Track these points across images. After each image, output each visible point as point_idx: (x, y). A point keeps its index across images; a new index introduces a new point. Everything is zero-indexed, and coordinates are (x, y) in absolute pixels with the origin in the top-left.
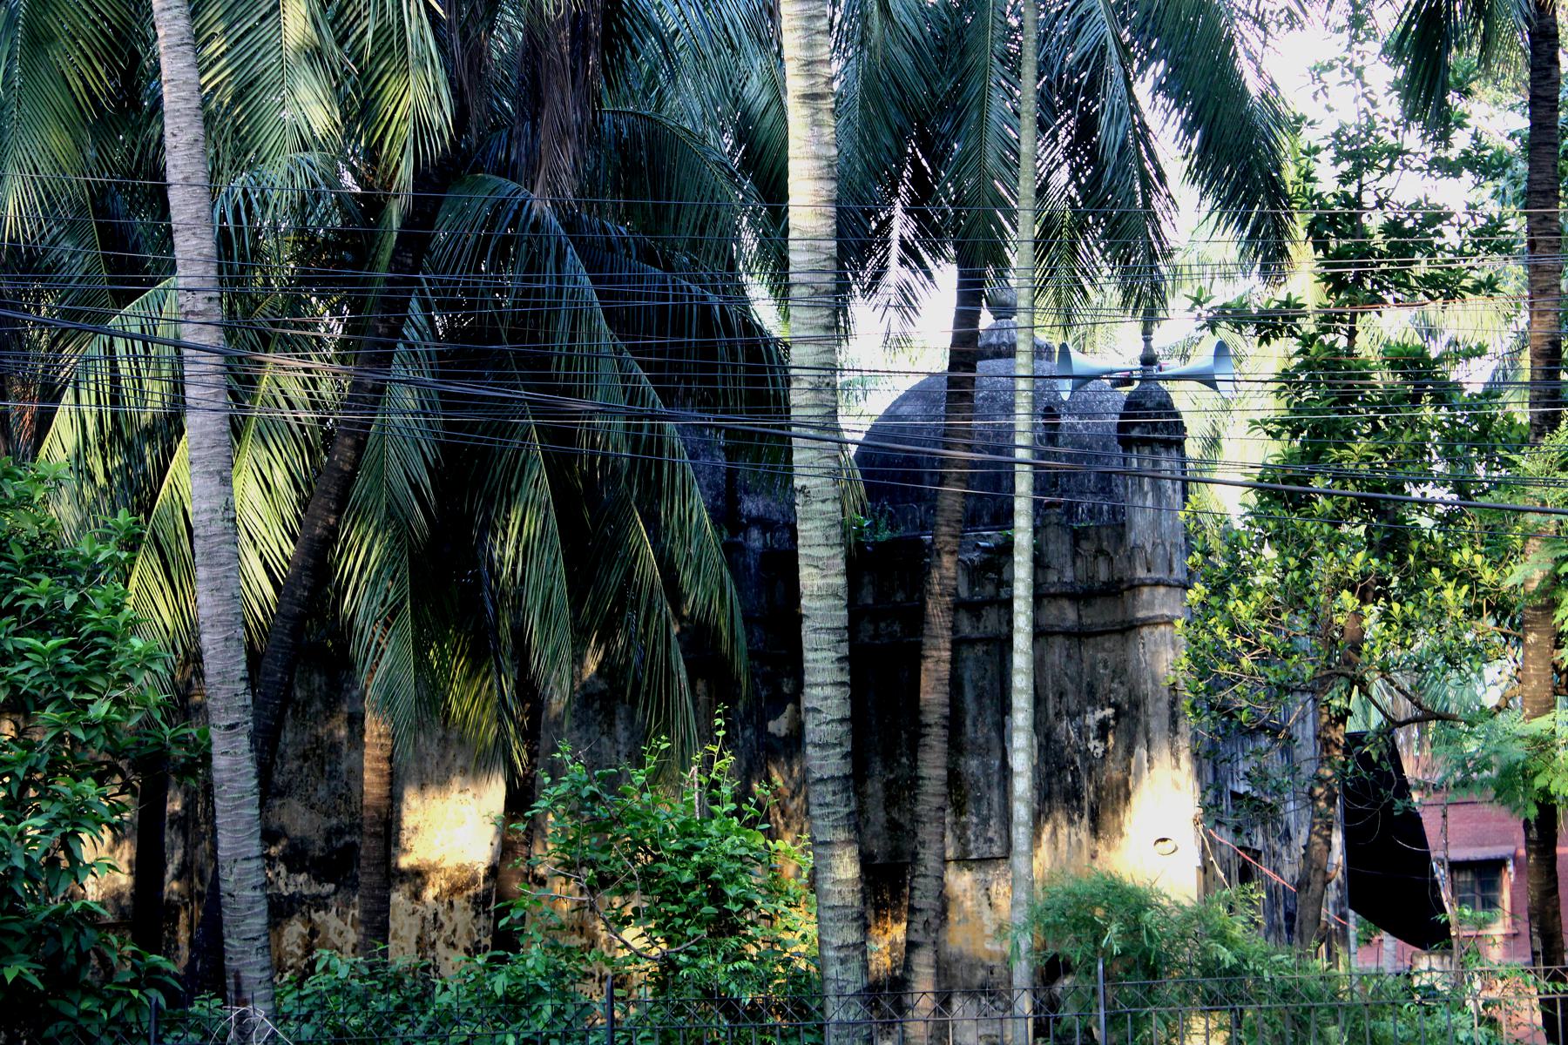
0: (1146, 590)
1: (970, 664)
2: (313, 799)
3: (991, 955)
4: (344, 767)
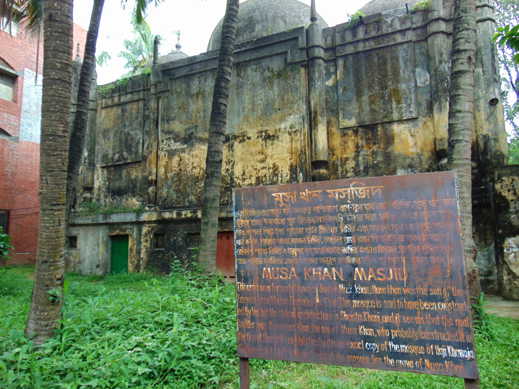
2: (182, 120)
3: (412, 154)
4: (190, 110)
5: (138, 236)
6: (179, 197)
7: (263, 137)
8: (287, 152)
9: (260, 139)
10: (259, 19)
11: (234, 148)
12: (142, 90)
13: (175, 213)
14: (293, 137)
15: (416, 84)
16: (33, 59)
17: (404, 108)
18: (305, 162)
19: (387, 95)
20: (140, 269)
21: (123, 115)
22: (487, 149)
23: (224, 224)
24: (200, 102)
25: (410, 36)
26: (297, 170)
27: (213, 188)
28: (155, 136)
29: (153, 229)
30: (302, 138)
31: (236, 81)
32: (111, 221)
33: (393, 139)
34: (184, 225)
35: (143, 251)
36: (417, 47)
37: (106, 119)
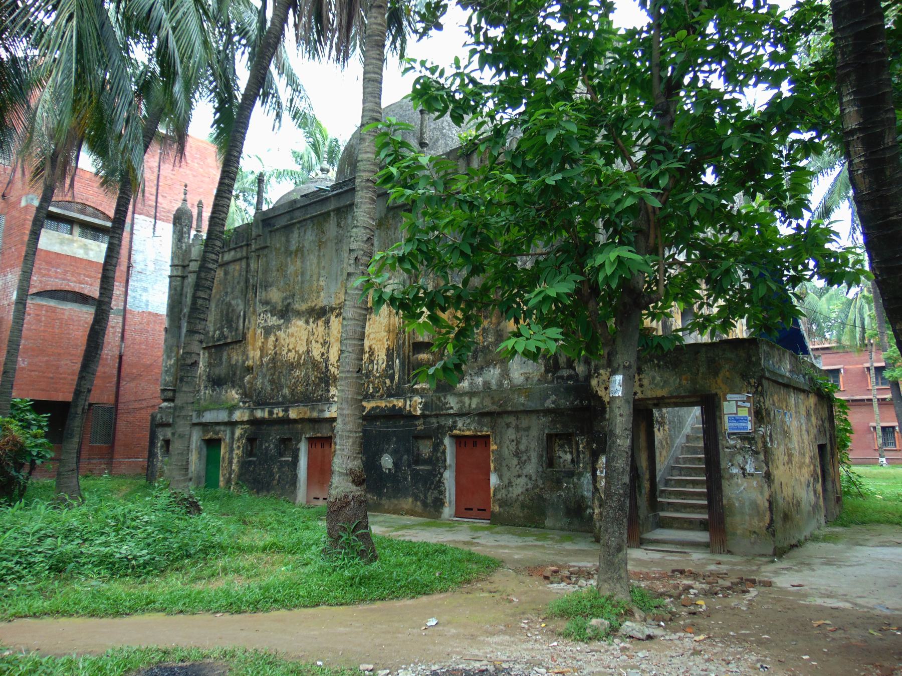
6: (272, 390)
8: (385, 331)
13: (267, 410)
16: (150, 203)
18: (404, 343)
21: (226, 279)
24: (298, 263)
27: (182, 394)
29: (245, 432)
32: (204, 420)
34: (276, 427)
35: (235, 461)
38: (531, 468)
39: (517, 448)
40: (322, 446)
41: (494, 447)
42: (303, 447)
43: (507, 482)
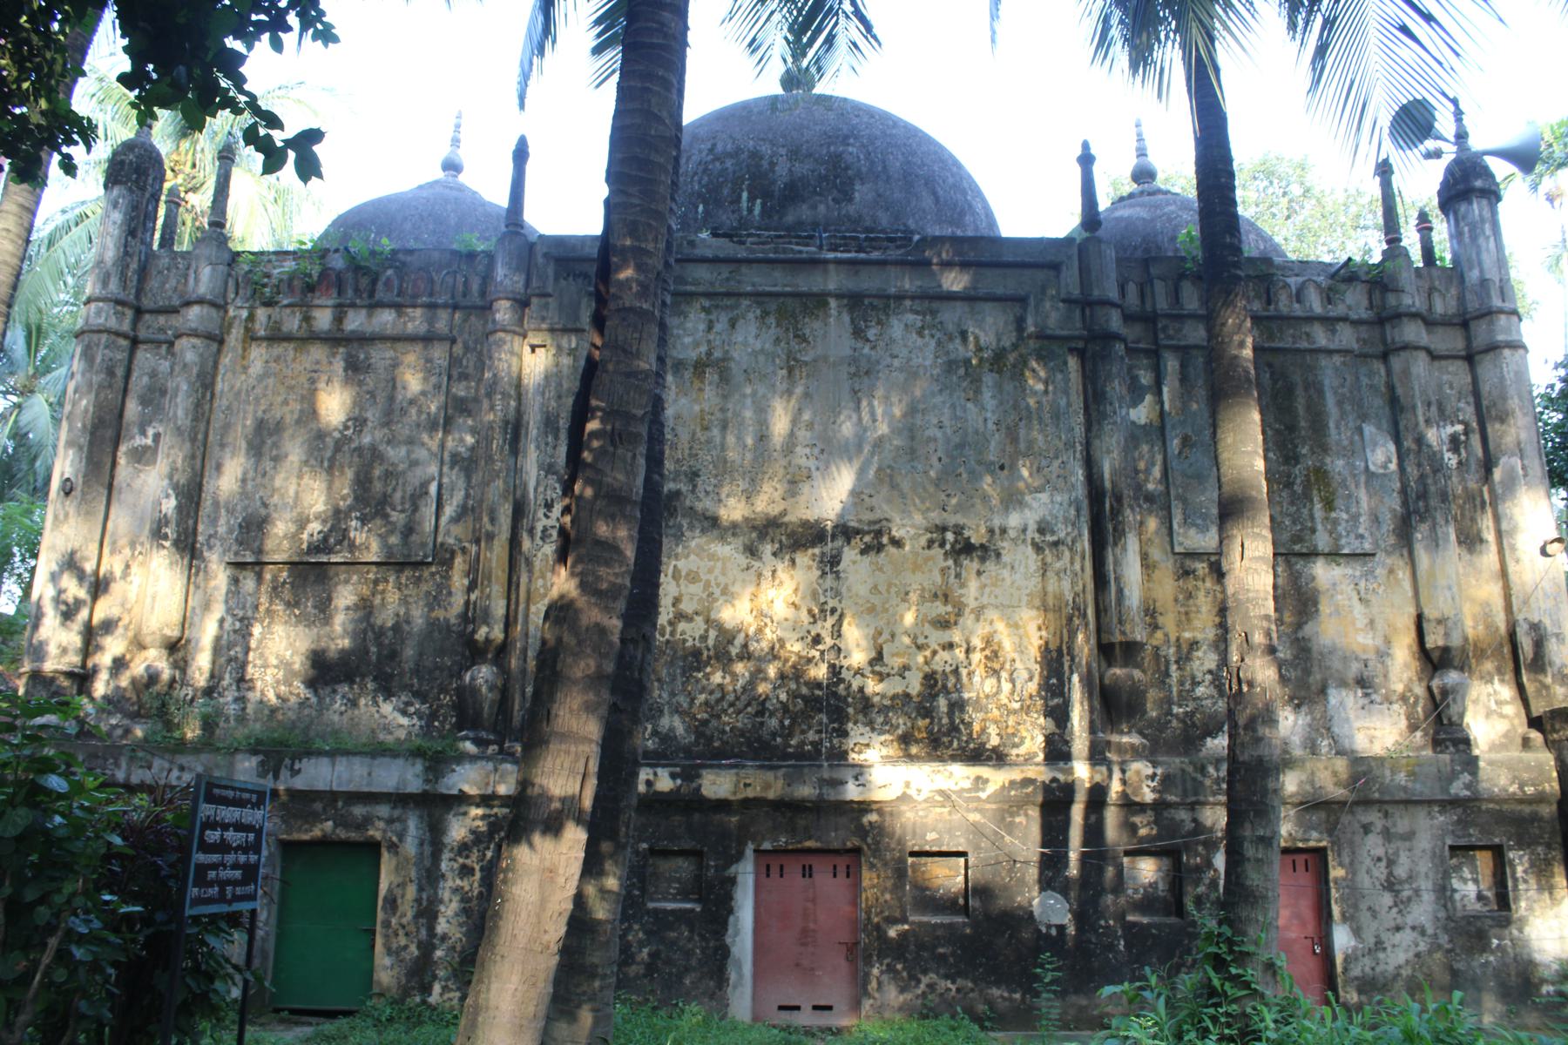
0: (1503, 317)
1: (1329, 372)
3: (1365, 649)
5: (427, 849)
7: (948, 547)
8: (1030, 605)
9: (937, 552)
10: (864, 169)
11: (840, 568)
12: (445, 306)
14: (1049, 560)
15: (1367, 467)
17: (1344, 524)
19: (1298, 481)
20: (435, 977)
22: (1543, 657)
23: (801, 822)
25: (1347, 337)
26: (1062, 665)
28: (505, 482)
30: (1077, 567)
31: (848, 352)
33: (1316, 603)
36: (1363, 370)
37: (271, 381)
38: (1423, 912)
39: (1390, 874)
40: (807, 872)
41: (1336, 873)
42: (746, 874)
43: (1372, 940)
